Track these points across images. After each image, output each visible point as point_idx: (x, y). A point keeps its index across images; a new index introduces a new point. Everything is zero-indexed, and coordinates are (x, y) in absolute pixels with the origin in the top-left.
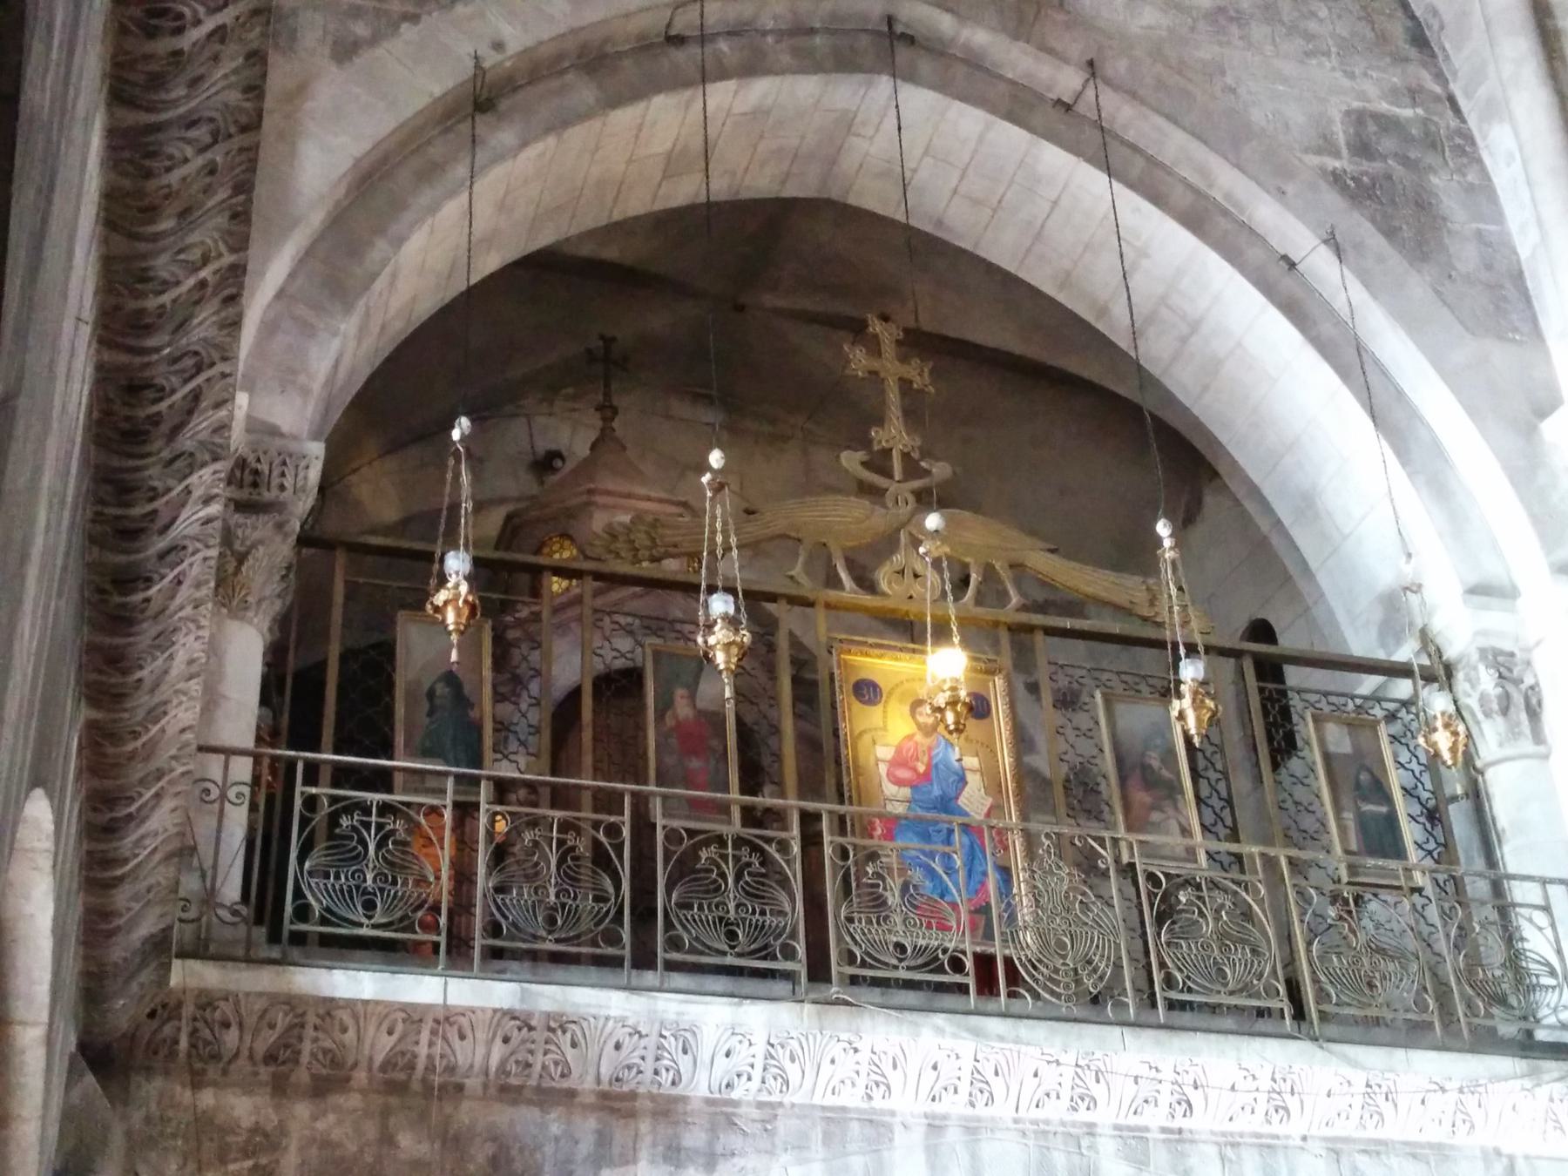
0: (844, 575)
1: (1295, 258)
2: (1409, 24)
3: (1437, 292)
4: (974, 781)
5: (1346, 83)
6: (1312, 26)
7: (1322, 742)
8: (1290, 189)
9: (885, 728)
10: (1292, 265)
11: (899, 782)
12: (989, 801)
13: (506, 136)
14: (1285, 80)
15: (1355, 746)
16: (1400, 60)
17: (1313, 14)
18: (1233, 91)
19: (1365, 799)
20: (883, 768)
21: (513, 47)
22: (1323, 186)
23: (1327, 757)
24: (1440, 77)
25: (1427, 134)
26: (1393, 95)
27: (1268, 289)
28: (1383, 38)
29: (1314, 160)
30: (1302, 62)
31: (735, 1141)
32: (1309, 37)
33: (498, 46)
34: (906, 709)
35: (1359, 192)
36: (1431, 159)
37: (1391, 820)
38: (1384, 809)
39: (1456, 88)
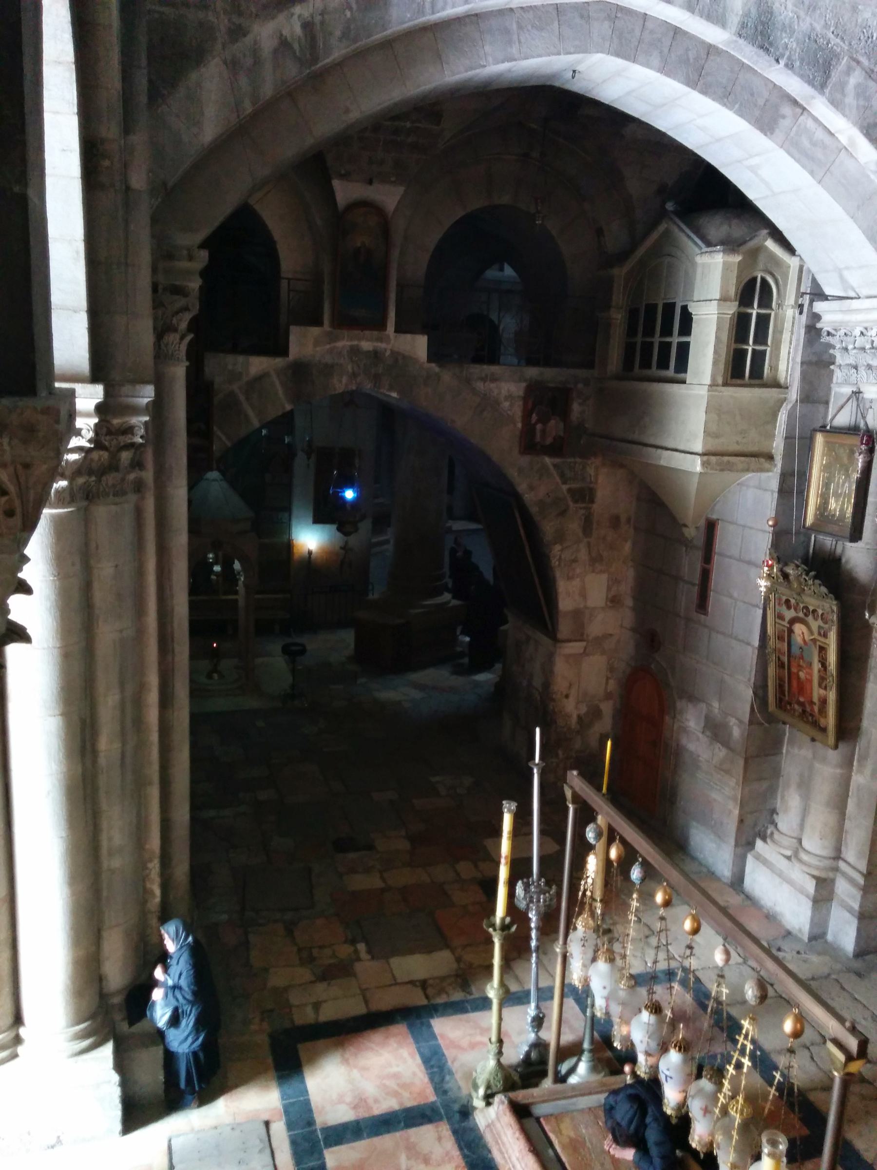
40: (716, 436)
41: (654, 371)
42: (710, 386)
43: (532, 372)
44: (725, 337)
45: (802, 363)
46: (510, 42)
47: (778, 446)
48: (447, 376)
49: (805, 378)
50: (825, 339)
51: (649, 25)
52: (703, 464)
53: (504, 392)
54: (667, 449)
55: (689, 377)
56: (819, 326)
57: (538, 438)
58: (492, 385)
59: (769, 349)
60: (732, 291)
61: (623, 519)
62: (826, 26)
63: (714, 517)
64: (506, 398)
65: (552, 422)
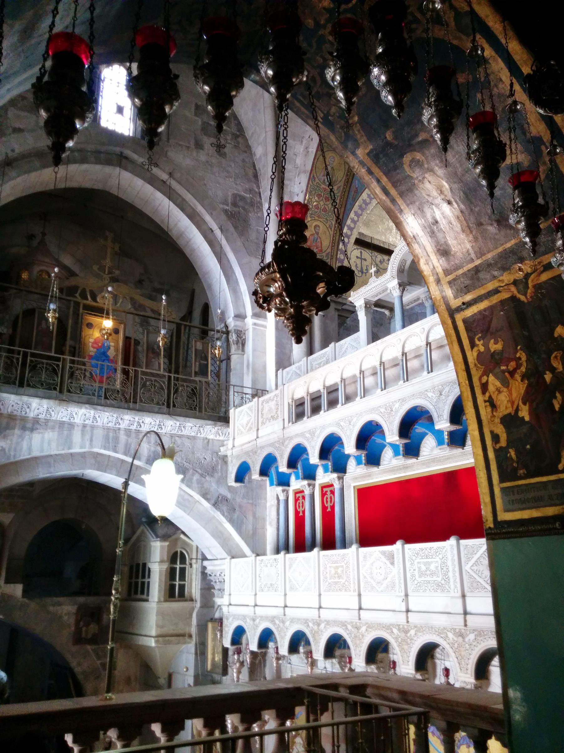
0: (89, 297)
1: (213, 230)
2: (254, 171)
3: (244, 244)
4: (112, 348)
5: (235, 186)
6: (230, 169)
7: (195, 346)
8: (214, 213)
9: (93, 335)
10: (212, 231)
11: (94, 348)
12: (115, 354)
13: (13, 173)
14: (219, 184)
15: (203, 348)
16: (249, 181)
17: (231, 166)
18: (205, 185)
19: (202, 360)
20: (90, 344)
21: (17, 151)
22: (222, 213)
23: (196, 350)
24: (258, 187)
25: (252, 202)
26: (245, 191)
27: (205, 237)
28: (246, 175)
29: (221, 206)
30: (224, 179)
31: (38, 426)
32: (228, 172)
33: (13, 151)
34: (98, 331)
35: (231, 216)
36: (251, 209)
37: (207, 365)
38: (206, 363)
39: (261, 190)
40: (162, 627)
41: (139, 596)
42: (158, 602)
43: (81, 599)
44: (163, 579)
45: (201, 589)
46: (50, 467)
47: (194, 630)
48: (33, 605)
49: (202, 595)
50: (209, 578)
51: (111, 459)
52: (156, 642)
53: (65, 611)
54: (142, 635)
55: (150, 598)
56: (206, 572)
57: (83, 635)
58: (59, 608)
59: (186, 583)
60: (165, 558)
61: (133, 678)
62: (182, 459)
63: (171, 671)
64: (66, 614)
65: (92, 626)
